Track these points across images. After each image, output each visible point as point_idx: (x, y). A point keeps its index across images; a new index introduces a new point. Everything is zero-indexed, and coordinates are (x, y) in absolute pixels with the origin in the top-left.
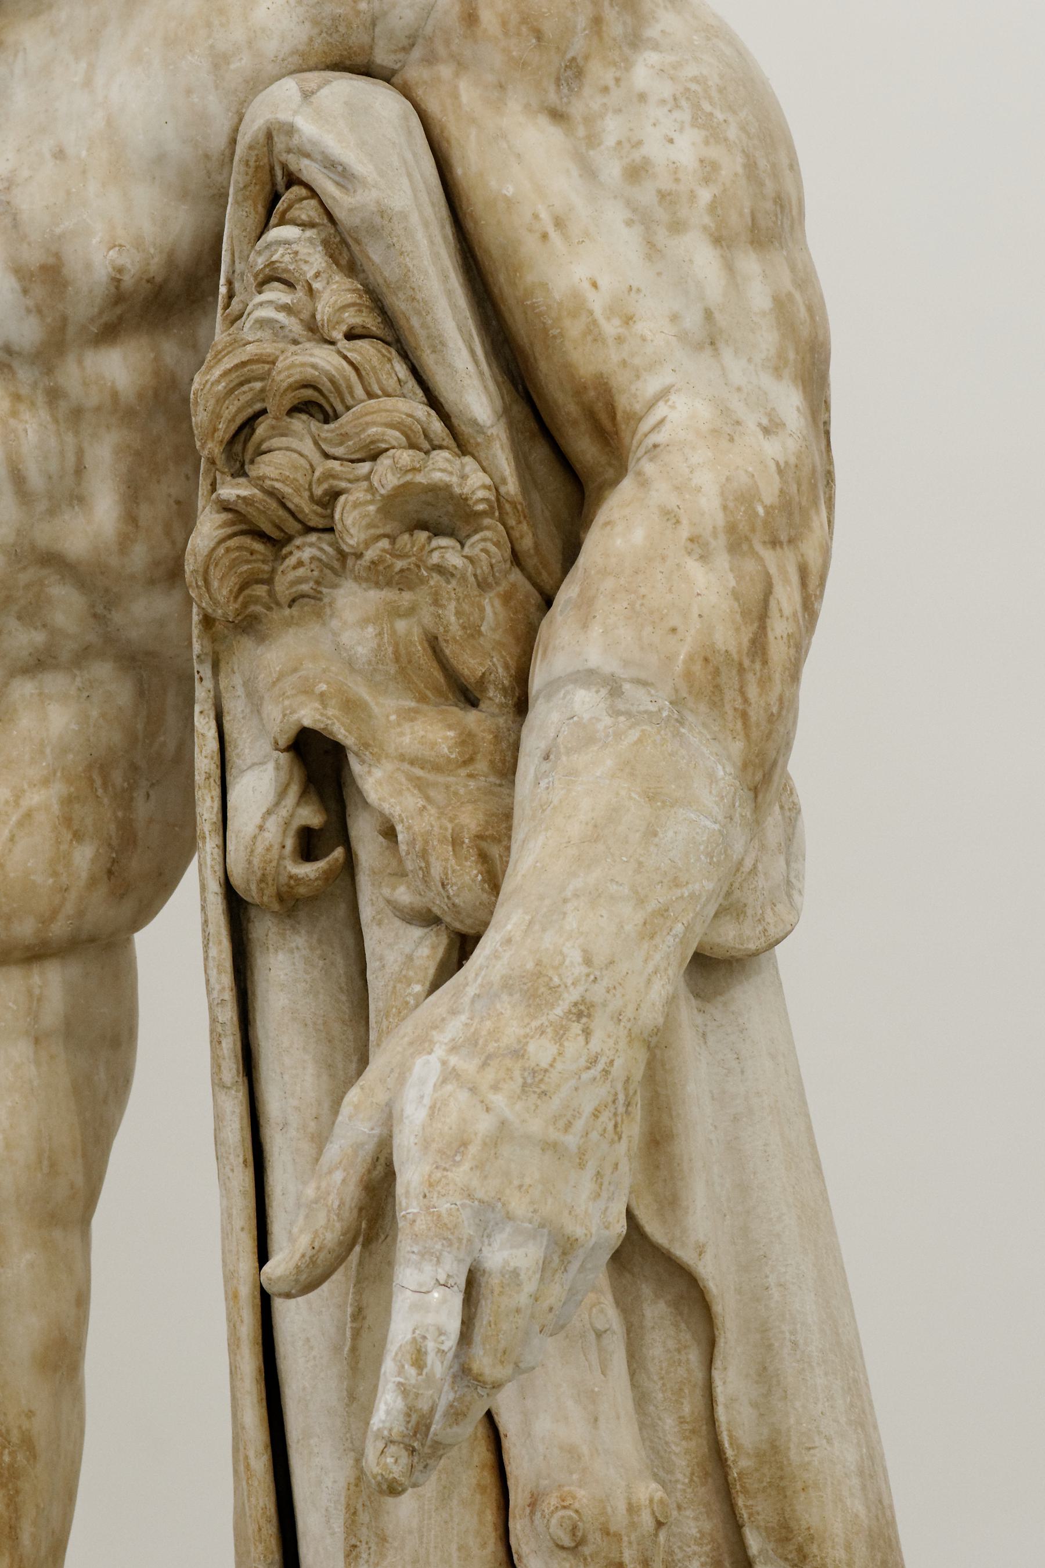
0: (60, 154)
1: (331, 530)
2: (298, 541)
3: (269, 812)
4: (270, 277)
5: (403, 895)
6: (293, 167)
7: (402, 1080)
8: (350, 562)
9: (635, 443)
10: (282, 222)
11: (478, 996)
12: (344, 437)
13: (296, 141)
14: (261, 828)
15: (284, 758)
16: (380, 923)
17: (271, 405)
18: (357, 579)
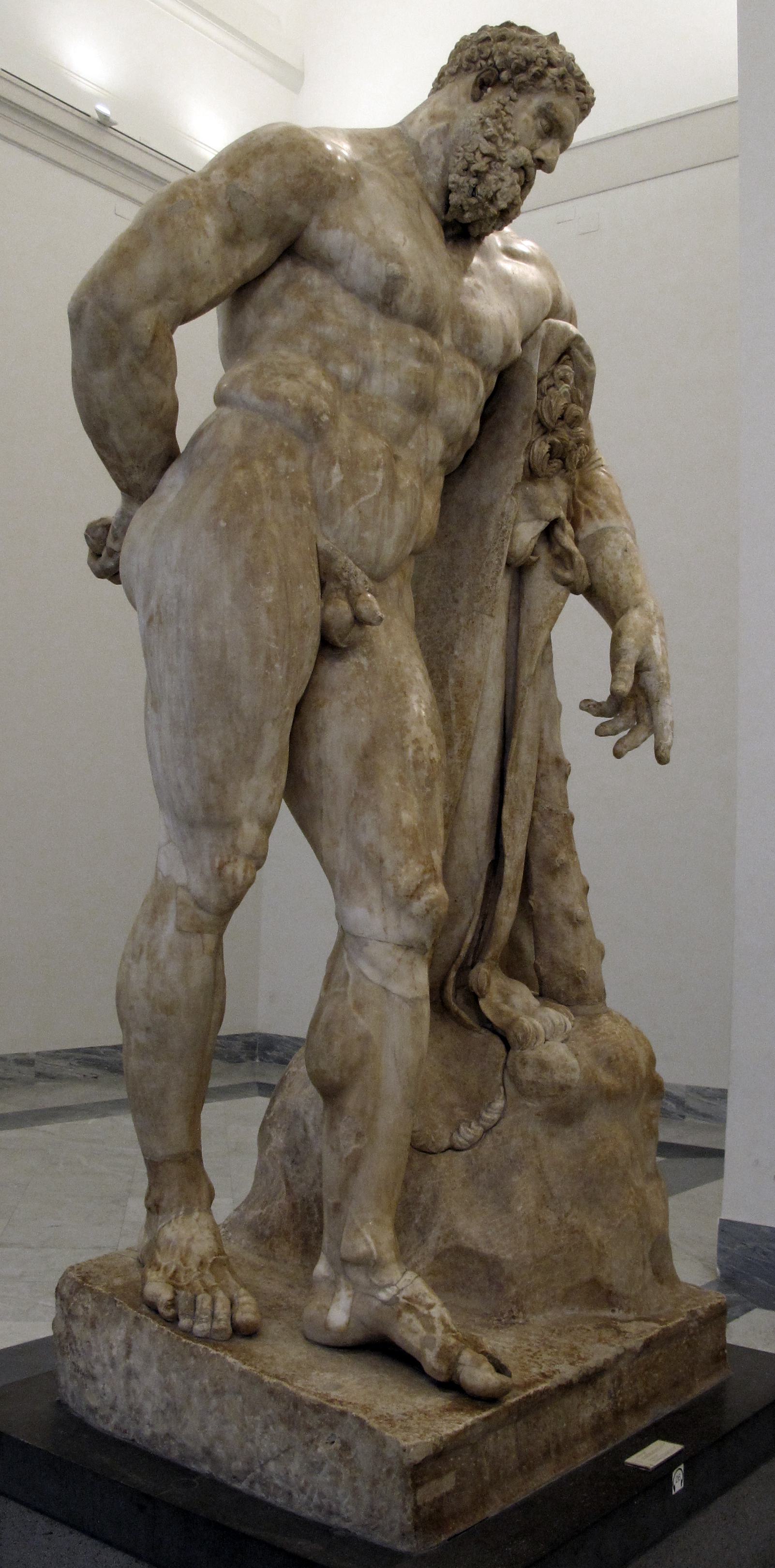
0: (510, 312)
1: (563, 460)
2: (555, 460)
3: (533, 538)
4: (564, 379)
5: (568, 575)
6: (576, 350)
7: (649, 641)
8: (563, 471)
9: (591, 461)
10: (564, 363)
11: (657, 621)
12: (578, 436)
13: (582, 344)
14: (531, 542)
15: (548, 523)
16: (548, 580)
17: (568, 419)
18: (562, 477)
